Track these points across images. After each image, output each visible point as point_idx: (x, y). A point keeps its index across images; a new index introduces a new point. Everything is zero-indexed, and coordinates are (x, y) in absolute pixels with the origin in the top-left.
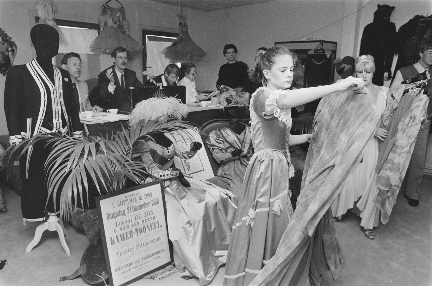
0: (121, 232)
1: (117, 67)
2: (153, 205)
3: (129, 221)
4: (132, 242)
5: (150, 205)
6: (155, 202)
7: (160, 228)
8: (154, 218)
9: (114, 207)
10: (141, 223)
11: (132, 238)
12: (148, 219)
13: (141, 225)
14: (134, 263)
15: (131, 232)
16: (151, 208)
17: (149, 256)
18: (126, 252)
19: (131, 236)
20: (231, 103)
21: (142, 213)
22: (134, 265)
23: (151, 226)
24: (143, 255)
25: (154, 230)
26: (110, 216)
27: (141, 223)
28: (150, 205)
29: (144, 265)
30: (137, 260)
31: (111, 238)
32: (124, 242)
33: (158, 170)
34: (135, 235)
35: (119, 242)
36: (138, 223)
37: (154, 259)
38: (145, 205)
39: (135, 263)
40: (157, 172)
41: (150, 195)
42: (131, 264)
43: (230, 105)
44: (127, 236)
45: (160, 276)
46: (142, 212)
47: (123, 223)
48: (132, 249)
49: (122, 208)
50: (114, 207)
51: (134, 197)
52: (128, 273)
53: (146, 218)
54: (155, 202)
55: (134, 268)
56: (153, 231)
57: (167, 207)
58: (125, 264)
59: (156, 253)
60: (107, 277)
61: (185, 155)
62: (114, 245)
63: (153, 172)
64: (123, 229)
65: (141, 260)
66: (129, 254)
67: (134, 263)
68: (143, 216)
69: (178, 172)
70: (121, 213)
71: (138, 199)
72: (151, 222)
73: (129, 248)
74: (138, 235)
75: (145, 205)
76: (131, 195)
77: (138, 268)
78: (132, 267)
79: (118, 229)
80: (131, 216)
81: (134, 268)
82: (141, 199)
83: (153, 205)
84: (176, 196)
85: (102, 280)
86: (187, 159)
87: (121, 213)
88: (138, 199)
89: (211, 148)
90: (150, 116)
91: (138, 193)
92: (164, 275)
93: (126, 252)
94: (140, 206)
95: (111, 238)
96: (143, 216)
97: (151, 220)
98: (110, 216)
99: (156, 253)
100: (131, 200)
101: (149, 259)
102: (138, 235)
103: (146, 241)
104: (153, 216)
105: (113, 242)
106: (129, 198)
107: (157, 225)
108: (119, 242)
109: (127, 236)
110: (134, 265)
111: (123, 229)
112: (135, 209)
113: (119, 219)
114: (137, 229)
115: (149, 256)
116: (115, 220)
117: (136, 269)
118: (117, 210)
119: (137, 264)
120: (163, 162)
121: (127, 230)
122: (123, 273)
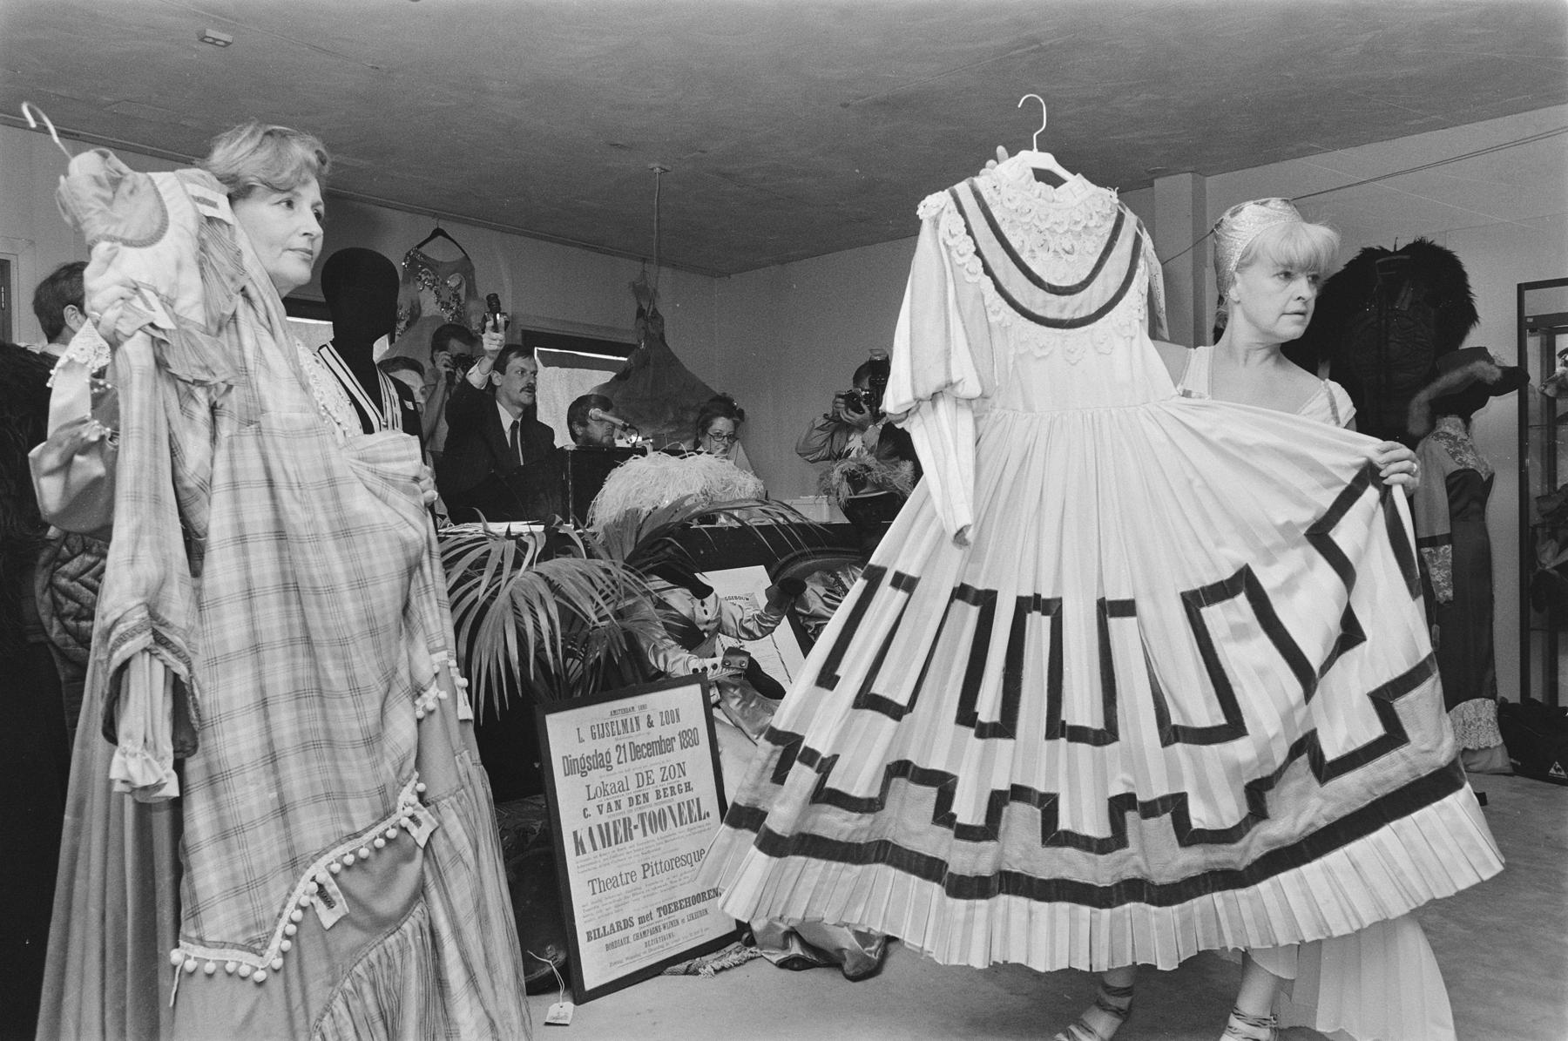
0: (603, 819)
1: (504, 399)
2: (683, 746)
3: (622, 787)
4: (630, 854)
5: (677, 745)
6: (688, 739)
7: (703, 822)
8: (688, 788)
9: (581, 741)
10: (652, 796)
11: (630, 843)
12: (673, 793)
13: (653, 806)
14: (636, 921)
15: (627, 822)
16: (677, 755)
17: (678, 906)
18: (614, 882)
19: (629, 836)
20: (863, 486)
21: (656, 769)
22: (636, 929)
23: (681, 814)
24: (661, 899)
25: (690, 825)
26: (572, 767)
27: (652, 796)
28: (677, 745)
29: (665, 932)
30: (644, 913)
31: (575, 833)
32: (608, 849)
33: (685, 654)
34: (637, 833)
35: (595, 849)
36: (646, 797)
37: (692, 917)
38: (663, 746)
39: (641, 920)
40: (680, 661)
41: (672, 716)
42: (628, 923)
43: (866, 493)
44: (616, 833)
45: (717, 965)
46: (655, 763)
47: (605, 792)
48: (632, 874)
49: (607, 744)
50: (581, 741)
51: (632, 715)
52: (621, 952)
53: (666, 784)
54: (688, 739)
55: (637, 937)
56: (685, 827)
57: (722, 758)
58: (613, 919)
59: (697, 899)
60: (561, 957)
61: (750, 626)
62: (582, 857)
63: (671, 660)
64: (605, 808)
65: (655, 914)
66: (622, 889)
67: (636, 921)
68: (657, 776)
69: (745, 659)
70: (601, 761)
71: (643, 723)
72: (678, 798)
73: (625, 870)
74: (645, 834)
75: (663, 746)
76: (625, 711)
77: (649, 938)
78: (630, 932)
79: (593, 810)
80: (627, 770)
81: (637, 937)
82: (650, 725)
83: (683, 746)
84: (744, 726)
85: (548, 969)
86: (757, 638)
87: (601, 761)
88: (643, 723)
89: (812, 624)
90: (656, 497)
91: (643, 707)
92: (725, 963)
93: (614, 882)
94: (649, 746)
95: (575, 833)
96: (657, 776)
97: (680, 791)
98: (572, 767)
99: (697, 899)
100: (624, 724)
101: (678, 915)
102: (645, 834)
103: (668, 857)
104: (683, 780)
105: (579, 846)
106: (619, 718)
107: (695, 810)
108: (595, 849)
109: (616, 833)
110: (636, 929)
111: (605, 808)
112: (637, 752)
113: (596, 777)
114: (642, 816)
115: (678, 906)
116: (586, 780)
117: (642, 941)
118: (589, 748)
119: (646, 926)
120: (691, 636)
121: (618, 816)
122: (608, 947)
